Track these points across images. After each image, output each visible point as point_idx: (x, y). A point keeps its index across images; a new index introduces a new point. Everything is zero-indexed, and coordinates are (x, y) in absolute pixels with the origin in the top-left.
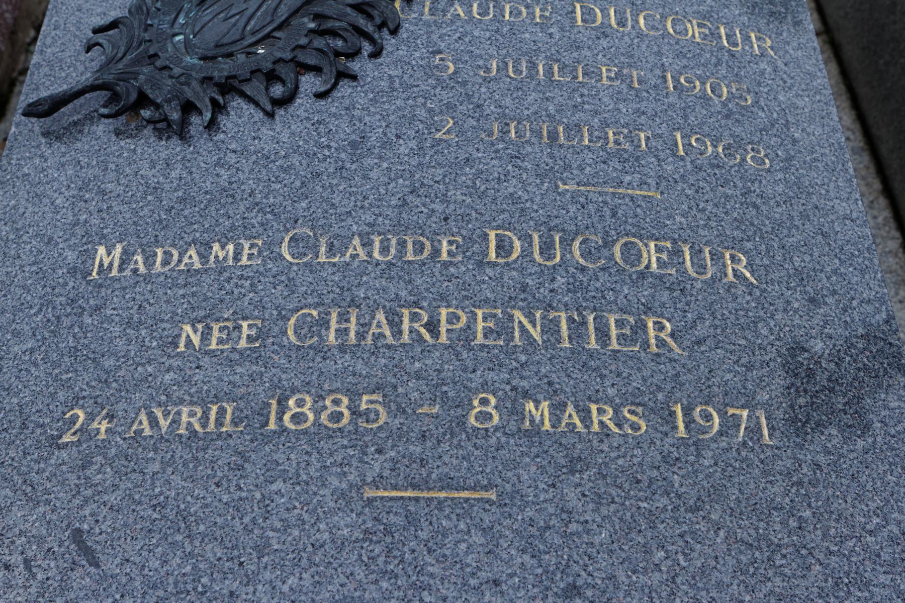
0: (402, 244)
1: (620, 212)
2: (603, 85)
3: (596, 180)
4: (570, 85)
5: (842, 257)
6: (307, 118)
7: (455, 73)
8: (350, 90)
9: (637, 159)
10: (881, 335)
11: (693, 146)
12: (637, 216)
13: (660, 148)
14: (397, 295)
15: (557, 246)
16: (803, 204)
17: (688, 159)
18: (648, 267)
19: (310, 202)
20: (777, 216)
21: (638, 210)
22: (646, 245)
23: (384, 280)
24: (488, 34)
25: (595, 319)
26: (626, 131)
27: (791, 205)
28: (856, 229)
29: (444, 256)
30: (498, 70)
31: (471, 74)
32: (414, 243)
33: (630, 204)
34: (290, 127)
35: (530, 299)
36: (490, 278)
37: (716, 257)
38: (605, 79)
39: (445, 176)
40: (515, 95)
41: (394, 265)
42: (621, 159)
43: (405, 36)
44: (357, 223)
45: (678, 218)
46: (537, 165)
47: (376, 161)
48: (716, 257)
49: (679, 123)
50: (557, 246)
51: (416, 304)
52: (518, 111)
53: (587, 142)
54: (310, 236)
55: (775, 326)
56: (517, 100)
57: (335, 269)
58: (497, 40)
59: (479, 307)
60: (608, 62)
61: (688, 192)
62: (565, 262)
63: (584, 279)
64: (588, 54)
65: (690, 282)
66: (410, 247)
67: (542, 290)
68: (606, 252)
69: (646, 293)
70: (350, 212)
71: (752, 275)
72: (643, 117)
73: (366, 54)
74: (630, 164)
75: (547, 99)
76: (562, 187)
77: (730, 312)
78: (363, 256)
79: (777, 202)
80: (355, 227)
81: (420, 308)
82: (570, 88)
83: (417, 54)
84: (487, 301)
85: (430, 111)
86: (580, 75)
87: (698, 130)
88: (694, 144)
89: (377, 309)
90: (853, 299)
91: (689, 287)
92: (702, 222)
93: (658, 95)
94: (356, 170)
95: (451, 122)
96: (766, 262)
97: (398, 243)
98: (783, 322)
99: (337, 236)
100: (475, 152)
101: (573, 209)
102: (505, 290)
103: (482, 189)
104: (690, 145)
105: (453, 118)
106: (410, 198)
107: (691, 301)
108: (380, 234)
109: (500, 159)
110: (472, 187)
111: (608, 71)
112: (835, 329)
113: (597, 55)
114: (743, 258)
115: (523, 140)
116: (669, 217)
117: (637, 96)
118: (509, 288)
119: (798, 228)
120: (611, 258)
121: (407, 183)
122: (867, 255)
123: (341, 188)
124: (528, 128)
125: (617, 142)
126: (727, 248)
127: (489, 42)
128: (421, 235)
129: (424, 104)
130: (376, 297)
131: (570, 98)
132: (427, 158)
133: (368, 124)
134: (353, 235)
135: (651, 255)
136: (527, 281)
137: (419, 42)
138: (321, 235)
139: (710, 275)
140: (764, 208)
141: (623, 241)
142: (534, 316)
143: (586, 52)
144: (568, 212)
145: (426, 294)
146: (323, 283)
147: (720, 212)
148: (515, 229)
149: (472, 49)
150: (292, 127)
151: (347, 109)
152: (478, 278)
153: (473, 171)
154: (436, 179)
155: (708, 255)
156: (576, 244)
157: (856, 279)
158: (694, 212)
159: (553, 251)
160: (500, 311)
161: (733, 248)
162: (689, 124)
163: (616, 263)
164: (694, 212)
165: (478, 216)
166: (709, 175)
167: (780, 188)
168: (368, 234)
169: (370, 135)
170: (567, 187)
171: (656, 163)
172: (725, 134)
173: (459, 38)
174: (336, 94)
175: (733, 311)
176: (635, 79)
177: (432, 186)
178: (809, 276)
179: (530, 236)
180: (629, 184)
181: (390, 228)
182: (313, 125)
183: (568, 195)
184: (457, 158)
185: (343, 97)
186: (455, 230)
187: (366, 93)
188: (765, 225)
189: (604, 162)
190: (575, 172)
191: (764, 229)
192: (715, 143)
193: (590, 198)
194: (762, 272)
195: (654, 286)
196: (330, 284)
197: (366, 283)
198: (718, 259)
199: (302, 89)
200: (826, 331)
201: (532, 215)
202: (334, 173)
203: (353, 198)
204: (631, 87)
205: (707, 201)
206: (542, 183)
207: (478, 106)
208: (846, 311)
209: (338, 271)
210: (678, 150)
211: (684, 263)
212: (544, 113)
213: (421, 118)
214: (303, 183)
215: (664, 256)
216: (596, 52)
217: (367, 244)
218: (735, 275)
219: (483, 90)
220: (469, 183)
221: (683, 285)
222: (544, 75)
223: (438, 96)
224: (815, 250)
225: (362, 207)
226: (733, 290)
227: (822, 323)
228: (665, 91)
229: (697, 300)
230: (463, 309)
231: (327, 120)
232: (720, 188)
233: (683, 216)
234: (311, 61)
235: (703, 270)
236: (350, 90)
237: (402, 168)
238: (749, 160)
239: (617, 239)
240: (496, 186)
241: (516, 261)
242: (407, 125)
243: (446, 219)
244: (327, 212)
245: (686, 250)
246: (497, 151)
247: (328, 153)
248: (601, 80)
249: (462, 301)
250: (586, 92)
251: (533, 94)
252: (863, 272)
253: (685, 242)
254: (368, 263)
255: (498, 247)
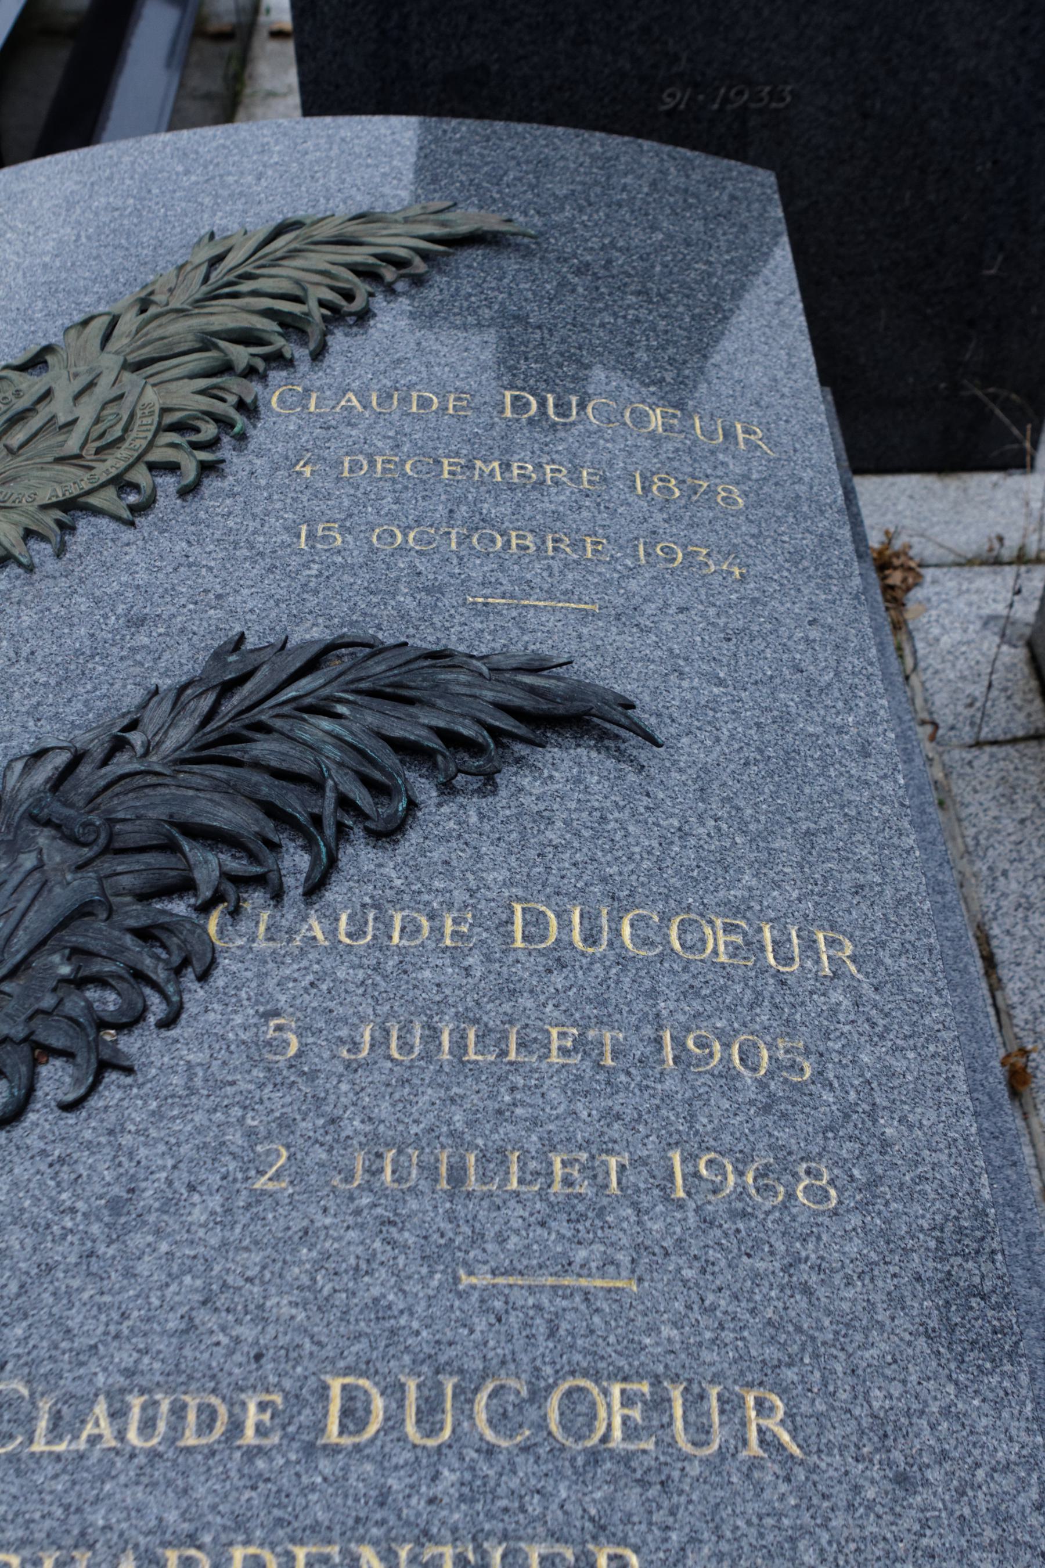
0: (179, 1411)
1: (564, 1326)
2: (551, 1065)
3: (525, 1262)
4: (494, 1069)
5: (962, 1378)
6: (43, 1153)
7: (300, 1054)
8: (119, 1095)
9: (601, 1213)
10: (1027, 1538)
11: (700, 1177)
12: (592, 1332)
13: (642, 1186)
14: (160, 1520)
15: (448, 1405)
16: (895, 1275)
17: (691, 1205)
18: (605, 1439)
19: (30, 1326)
20: (846, 1306)
21: (596, 1319)
22: (606, 1393)
23: (141, 1488)
24: (361, 974)
25: (504, 1556)
26: (584, 1156)
27: (872, 1280)
28: (990, 1313)
29: (249, 1436)
30: (372, 1046)
31: (326, 1055)
32: (200, 1409)
33: (583, 1307)
34: (11, 1171)
35: (392, 1520)
36: (325, 1479)
37: (730, 1405)
38: (554, 1052)
39: (264, 1268)
40: (397, 1096)
41: (160, 1455)
42: (573, 1216)
43: (221, 983)
44: (105, 1369)
45: (666, 1331)
46: (425, 1238)
47: (150, 1238)
48: (730, 1405)
49: (678, 1132)
50: (448, 1405)
51: (192, 1540)
52: (401, 1128)
53: (514, 1185)
54: (21, 1398)
55: (830, 1543)
56: (400, 1105)
57: (59, 1467)
58: (375, 985)
59: (302, 1543)
60: (563, 1018)
61: (687, 1273)
62: (459, 1439)
63: (491, 1473)
64: (530, 1004)
65: (679, 1465)
66: (192, 1417)
67: (414, 1501)
68: (532, 1413)
69: (598, 1495)
70: (95, 1346)
71: (794, 1438)
72: (616, 1126)
73: (152, 1020)
74: (588, 1224)
75: (453, 1100)
76: (466, 1280)
77: (749, 1523)
78: (110, 1441)
79: (847, 1277)
80: (101, 1378)
81: (199, 1548)
82: (492, 1074)
83: (238, 1019)
84: (315, 1528)
85: (250, 1133)
86: (513, 1047)
87: (712, 1143)
88: (704, 1172)
89: (124, 1550)
90: (978, 1465)
91: (676, 1474)
92: (708, 1335)
93: (646, 1077)
94: (114, 1258)
95: (285, 1154)
96: (820, 1407)
97: (173, 1411)
98: (846, 1533)
99: (69, 1398)
100: (319, 1216)
101: (480, 1324)
102: (350, 1502)
103: (326, 1292)
104: (696, 1174)
105: (288, 1147)
106: (202, 1316)
107: (678, 1507)
108: (142, 1392)
109: (362, 1227)
110: (309, 1288)
111: (563, 1035)
112: (941, 1536)
113: (544, 1005)
114: (779, 1403)
115: (405, 1186)
116: (652, 1329)
117: (608, 1083)
118: (356, 1500)
119: (882, 1325)
120: (541, 1425)
121: (199, 1283)
122: (1008, 1367)
123: (85, 1296)
124: (415, 1160)
125: (568, 1182)
126: (750, 1385)
127: (360, 991)
128: (214, 1391)
129: (241, 1121)
130: (124, 1525)
131: (492, 1096)
132: (238, 1230)
133: (144, 1162)
134: (96, 1395)
135: (613, 1413)
136: (390, 1482)
137: (243, 994)
138: (43, 1395)
139: (715, 1446)
140: (822, 1292)
141: (564, 1386)
142: (396, 1555)
143: (526, 1001)
144: (472, 1331)
145: (210, 1518)
146: (35, 1496)
147: (741, 1311)
148: (376, 1372)
149: (331, 1005)
150: (16, 1171)
151: (111, 1132)
152: (305, 1480)
153: (314, 1254)
154: (249, 1274)
155: (715, 1403)
156: (482, 1398)
157: (984, 1421)
158: (695, 1315)
159: (439, 1417)
160: (337, 1549)
161: (761, 1384)
162: (697, 1132)
163: (550, 1434)
164: (695, 1315)
165: (315, 1348)
166: (726, 1235)
167: (852, 1248)
168: (123, 1391)
169: (143, 1185)
170: (474, 1280)
171: (633, 1219)
172: (760, 1146)
173: (312, 984)
174: (94, 1102)
175: (755, 1520)
176: (608, 1048)
177: (240, 1288)
178: (897, 1428)
179: (402, 1386)
180: (582, 1266)
181: (161, 1379)
182: (51, 1165)
183: (475, 1297)
184: (289, 1228)
185: (106, 1108)
186: (272, 1379)
187: (145, 1099)
188: (821, 1329)
189: (543, 1224)
190: (489, 1247)
191: (820, 1337)
192: (740, 1167)
193: (512, 1299)
194: (812, 1429)
195: (613, 1479)
196: (49, 1498)
197: (110, 1495)
198: (734, 1411)
199: (39, 1093)
200: (925, 1541)
201: (409, 1341)
202: (77, 1265)
203: (103, 1318)
204: (598, 1066)
205: (720, 1290)
206: (432, 1273)
207: (333, 1121)
208: (964, 1493)
209: (64, 1471)
210: (673, 1189)
211: (670, 1424)
212: (445, 1129)
213: (233, 1148)
214: (22, 1287)
215: (636, 1414)
216: (542, 998)
217: (119, 1414)
218: (762, 1442)
219: (344, 1087)
220: (305, 1280)
221: (666, 1470)
222: (451, 1053)
223: (267, 1103)
224: (911, 1369)
225: (117, 1337)
226: (756, 1474)
227: (916, 1527)
228: (659, 1068)
229: (690, 1502)
230: (273, 1546)
231: (75, 1156)
232: (745, 1259)
233: (675, 1324)
234: (57, 1041)
235: (703, 1437)
236: (119, 1095)
237: (192, 1253)
238: (800, 1195)
239: (555, 1384)
240: (351, 1284)
241: (373, 1440)
242: (209, 1165)
243: (258, 1357)
244: (56, 1347)
245: (676, 1395)
246: (358, 1212)
247: (69, 1224)
248: (547, 1056)
249: (272, 1531)
250: (521, 1082)
251: (430, 1091)
252: (998, 1405)
253: (675, 1379)
254: (117, 1453)
255: (346, 1412)
